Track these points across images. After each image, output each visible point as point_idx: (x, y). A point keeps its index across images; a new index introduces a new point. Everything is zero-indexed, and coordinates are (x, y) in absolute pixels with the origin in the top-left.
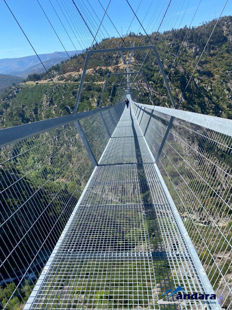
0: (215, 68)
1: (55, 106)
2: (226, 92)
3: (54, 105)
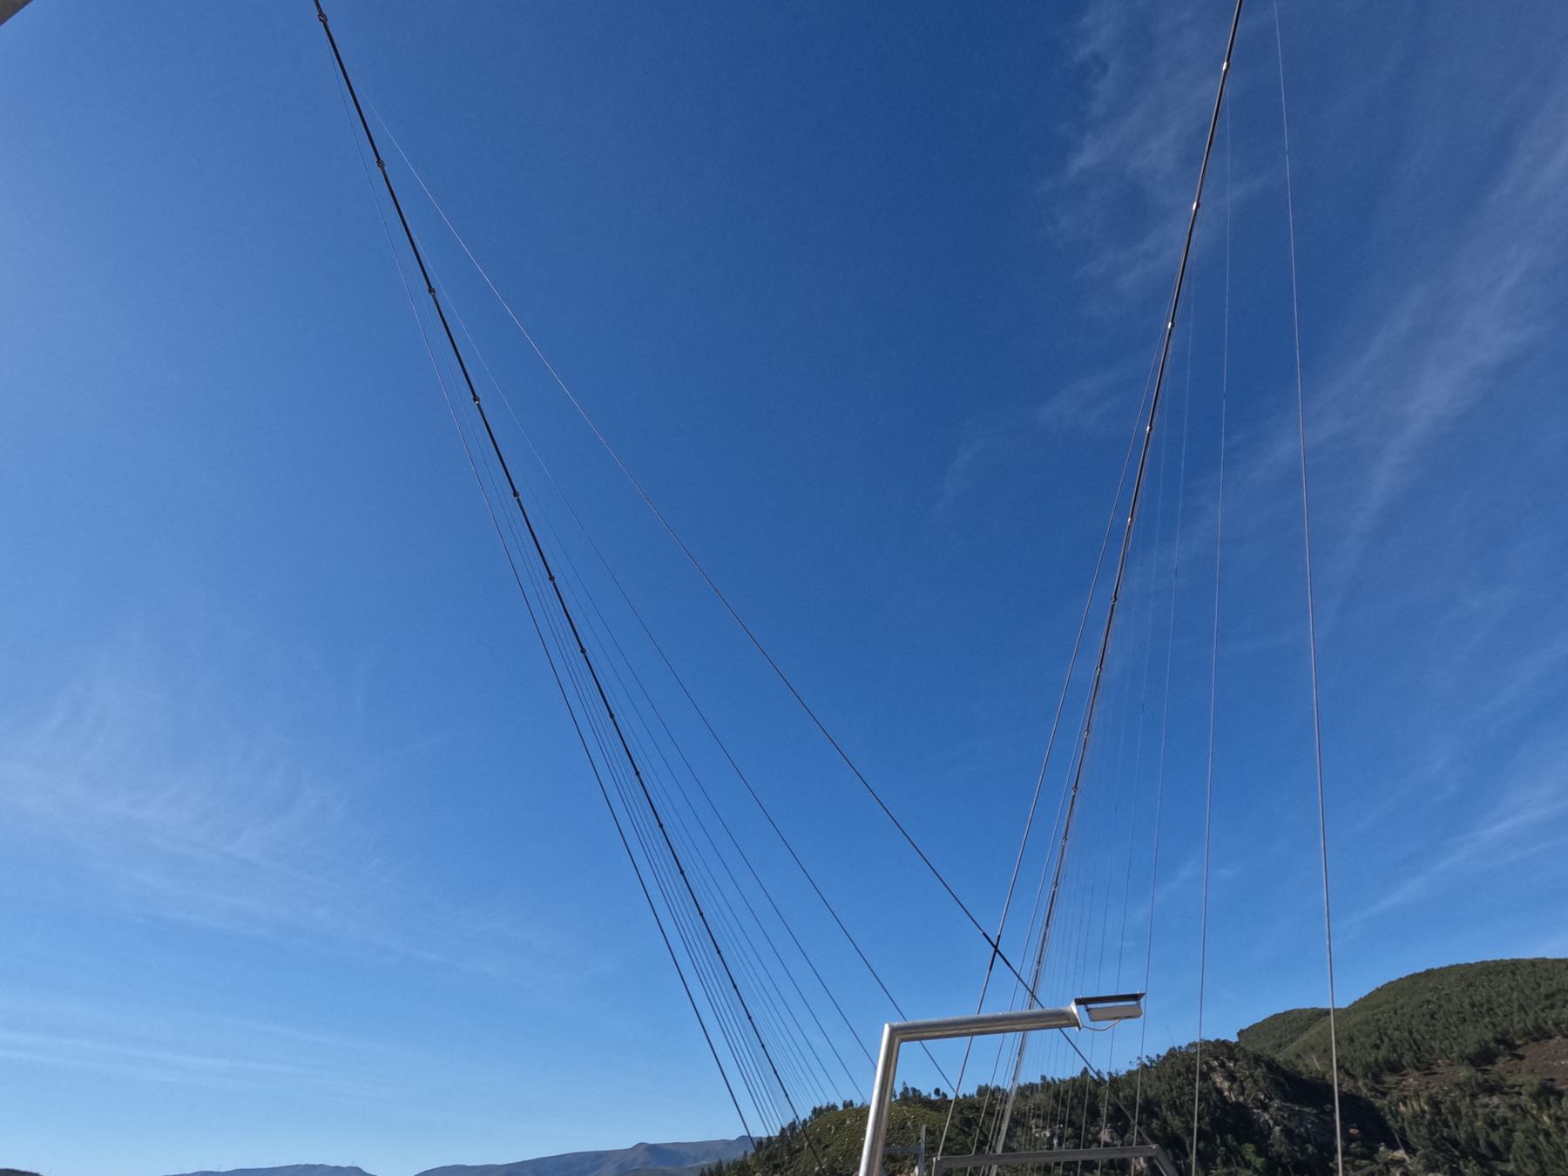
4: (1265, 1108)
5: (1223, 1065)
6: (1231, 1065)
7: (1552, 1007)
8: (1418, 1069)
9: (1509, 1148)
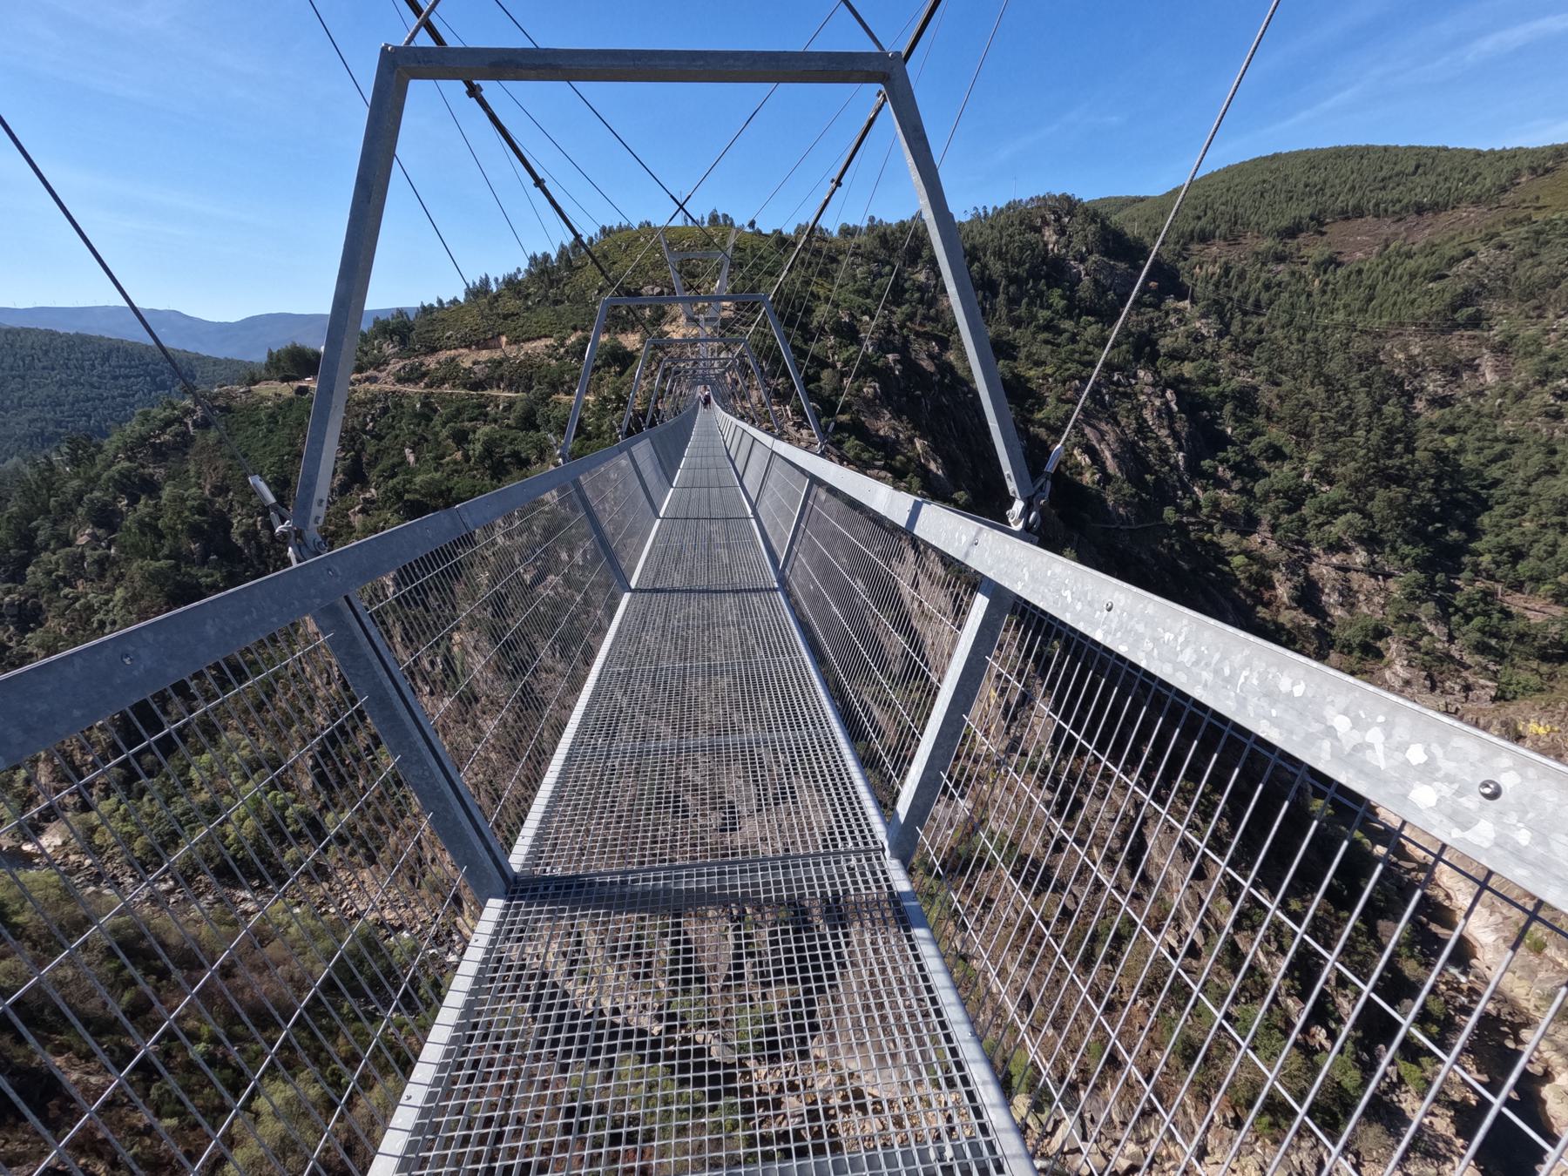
0: (1030, 369)
1: (368, 495)
3: (365, 484)
4: (1082, 260)
5: (1058, 220)
6: (1067, 220)
7: (1384, 188)
8: (1225, 239)
9: (1271, 302)
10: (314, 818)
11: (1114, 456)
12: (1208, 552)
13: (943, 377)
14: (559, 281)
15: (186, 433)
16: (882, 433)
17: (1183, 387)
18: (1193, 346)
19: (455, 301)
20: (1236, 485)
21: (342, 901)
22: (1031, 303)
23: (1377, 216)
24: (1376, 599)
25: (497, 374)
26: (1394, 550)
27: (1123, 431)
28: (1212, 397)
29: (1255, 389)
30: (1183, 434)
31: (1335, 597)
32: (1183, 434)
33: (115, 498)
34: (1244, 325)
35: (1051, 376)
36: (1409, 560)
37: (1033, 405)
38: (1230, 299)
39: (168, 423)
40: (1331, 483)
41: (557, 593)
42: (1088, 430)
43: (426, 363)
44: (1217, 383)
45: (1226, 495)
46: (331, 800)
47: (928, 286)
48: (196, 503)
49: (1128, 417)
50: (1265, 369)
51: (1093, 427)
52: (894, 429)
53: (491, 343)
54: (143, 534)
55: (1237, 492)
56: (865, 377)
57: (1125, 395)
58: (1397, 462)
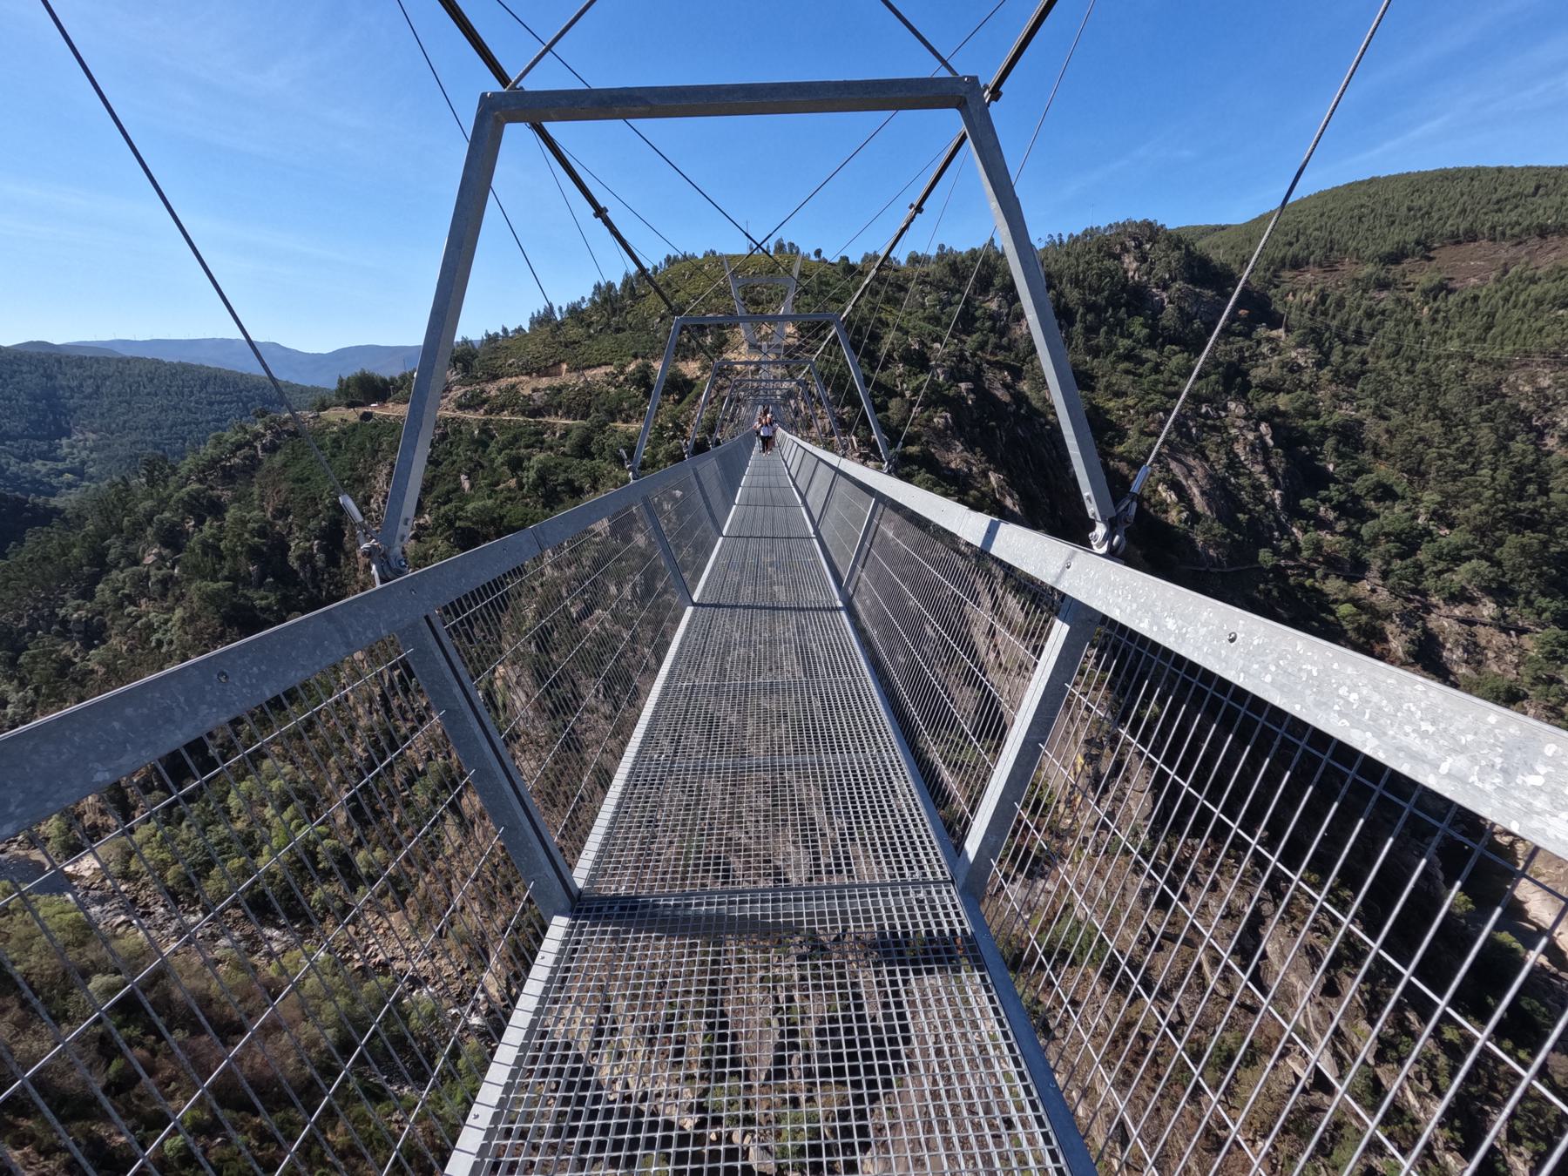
0: (1110, 400)
1: (422, 521)
2: (1164, 495)
4: (1165, 288)
5: (1139, 246)
6: (1148, 246)
7: (1500, 210)
8: (1320, 266)
9: (1375, 330)
10: (346, 855)
11: (1203, 493)
12: (1309, 599)
13: (1019, 407)
14: (622, 310)
15: (255, 457)
16: (953, 465)
17: (1277, 420)
18: (1289, 377)
19: (520, 330)
20: (1341, 526)
21: (367, 947)
22: (1110, 332)
23: (1493, 240)
24: (1508, 657)
25: (556, 402)
26: (1529, 603)
27: (1212, 466)
28: (1311, 431)
29: (1361, 423)
30: (1280, 471)
31: (1458, 653)
32: (1280, 471)
33: (183, 519)
34: (1346, 354)
35: (1133, 408)
36: (1546, 615)
37: (1113, 438)
38: (1328, 328)
39: (239, 446)
40: (1451, 526)
41: (605, 629)
42: (1173, 465)
43: (487, 390)
44: (1316, 416)
45: (1329, 537)
46: (365, 836)
47: (1000, 315)
48: (256, 526)
49: (1217, 452)
50: (1372, 402)
51: (1179, 461)
52: (966, 461)
53: (552, 371)
54: (205, 554)
55: (1341, 534)
56: (936, 407)
57: (1214, 428)
58: (1529, 504)
